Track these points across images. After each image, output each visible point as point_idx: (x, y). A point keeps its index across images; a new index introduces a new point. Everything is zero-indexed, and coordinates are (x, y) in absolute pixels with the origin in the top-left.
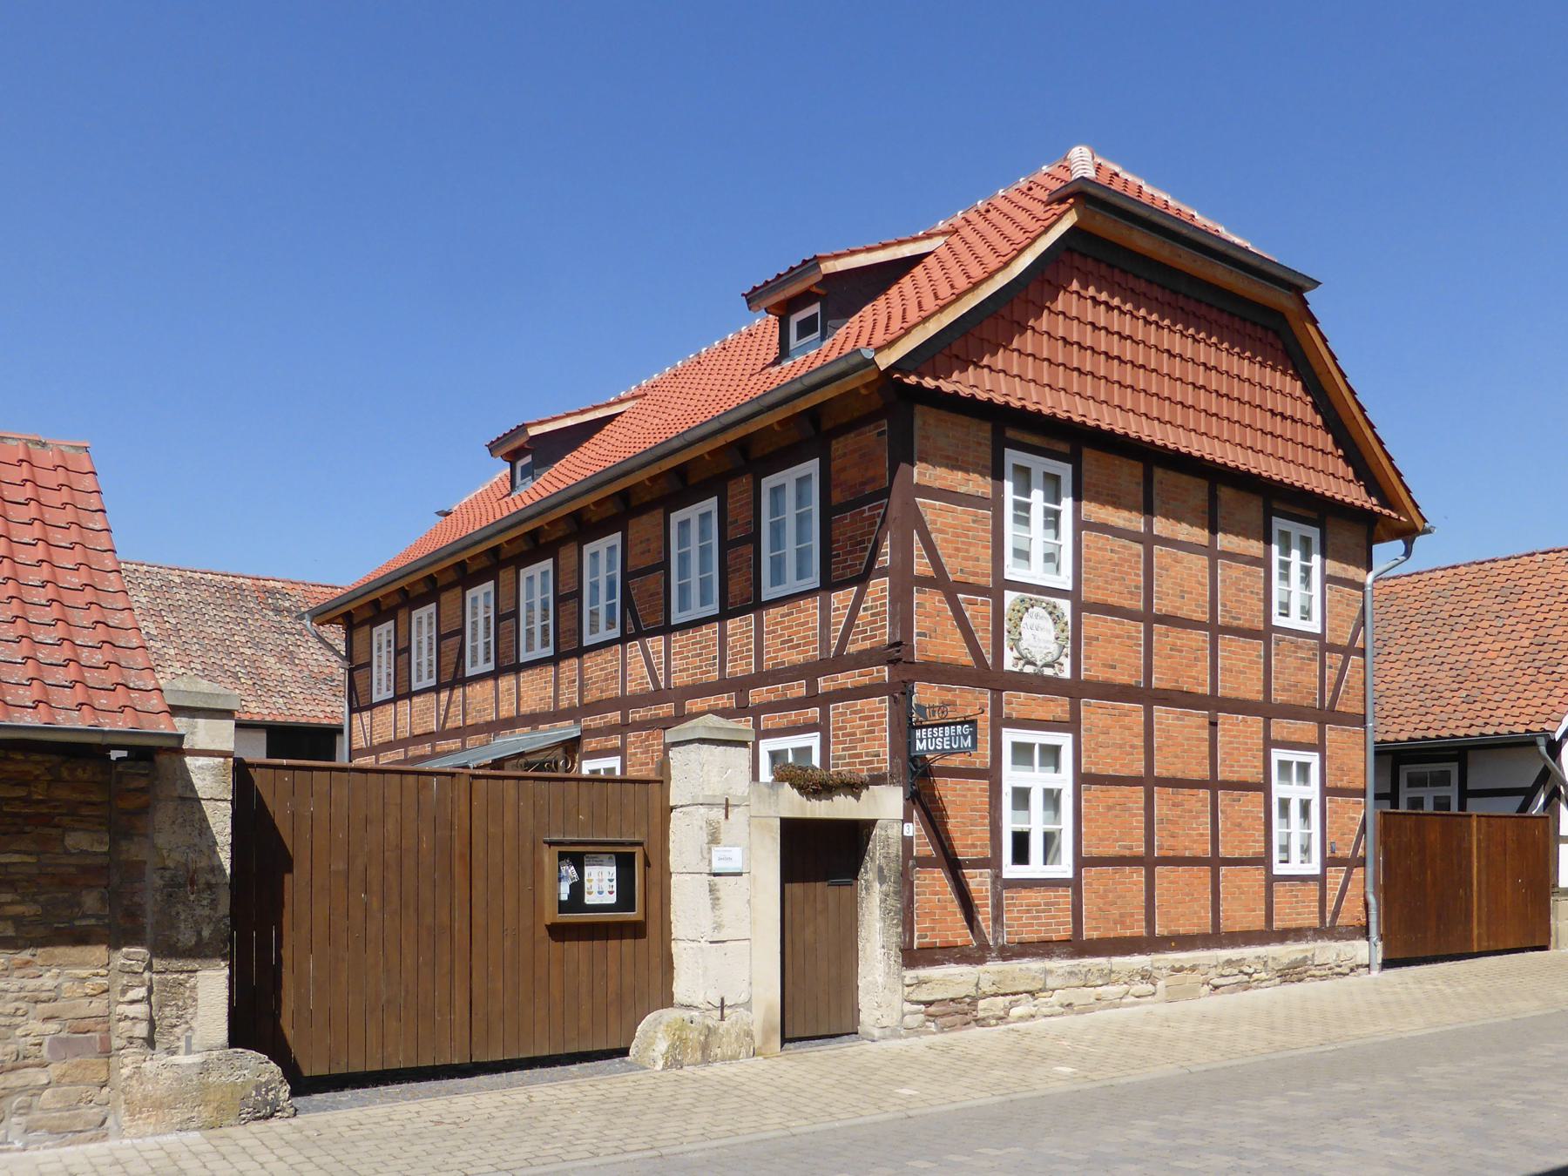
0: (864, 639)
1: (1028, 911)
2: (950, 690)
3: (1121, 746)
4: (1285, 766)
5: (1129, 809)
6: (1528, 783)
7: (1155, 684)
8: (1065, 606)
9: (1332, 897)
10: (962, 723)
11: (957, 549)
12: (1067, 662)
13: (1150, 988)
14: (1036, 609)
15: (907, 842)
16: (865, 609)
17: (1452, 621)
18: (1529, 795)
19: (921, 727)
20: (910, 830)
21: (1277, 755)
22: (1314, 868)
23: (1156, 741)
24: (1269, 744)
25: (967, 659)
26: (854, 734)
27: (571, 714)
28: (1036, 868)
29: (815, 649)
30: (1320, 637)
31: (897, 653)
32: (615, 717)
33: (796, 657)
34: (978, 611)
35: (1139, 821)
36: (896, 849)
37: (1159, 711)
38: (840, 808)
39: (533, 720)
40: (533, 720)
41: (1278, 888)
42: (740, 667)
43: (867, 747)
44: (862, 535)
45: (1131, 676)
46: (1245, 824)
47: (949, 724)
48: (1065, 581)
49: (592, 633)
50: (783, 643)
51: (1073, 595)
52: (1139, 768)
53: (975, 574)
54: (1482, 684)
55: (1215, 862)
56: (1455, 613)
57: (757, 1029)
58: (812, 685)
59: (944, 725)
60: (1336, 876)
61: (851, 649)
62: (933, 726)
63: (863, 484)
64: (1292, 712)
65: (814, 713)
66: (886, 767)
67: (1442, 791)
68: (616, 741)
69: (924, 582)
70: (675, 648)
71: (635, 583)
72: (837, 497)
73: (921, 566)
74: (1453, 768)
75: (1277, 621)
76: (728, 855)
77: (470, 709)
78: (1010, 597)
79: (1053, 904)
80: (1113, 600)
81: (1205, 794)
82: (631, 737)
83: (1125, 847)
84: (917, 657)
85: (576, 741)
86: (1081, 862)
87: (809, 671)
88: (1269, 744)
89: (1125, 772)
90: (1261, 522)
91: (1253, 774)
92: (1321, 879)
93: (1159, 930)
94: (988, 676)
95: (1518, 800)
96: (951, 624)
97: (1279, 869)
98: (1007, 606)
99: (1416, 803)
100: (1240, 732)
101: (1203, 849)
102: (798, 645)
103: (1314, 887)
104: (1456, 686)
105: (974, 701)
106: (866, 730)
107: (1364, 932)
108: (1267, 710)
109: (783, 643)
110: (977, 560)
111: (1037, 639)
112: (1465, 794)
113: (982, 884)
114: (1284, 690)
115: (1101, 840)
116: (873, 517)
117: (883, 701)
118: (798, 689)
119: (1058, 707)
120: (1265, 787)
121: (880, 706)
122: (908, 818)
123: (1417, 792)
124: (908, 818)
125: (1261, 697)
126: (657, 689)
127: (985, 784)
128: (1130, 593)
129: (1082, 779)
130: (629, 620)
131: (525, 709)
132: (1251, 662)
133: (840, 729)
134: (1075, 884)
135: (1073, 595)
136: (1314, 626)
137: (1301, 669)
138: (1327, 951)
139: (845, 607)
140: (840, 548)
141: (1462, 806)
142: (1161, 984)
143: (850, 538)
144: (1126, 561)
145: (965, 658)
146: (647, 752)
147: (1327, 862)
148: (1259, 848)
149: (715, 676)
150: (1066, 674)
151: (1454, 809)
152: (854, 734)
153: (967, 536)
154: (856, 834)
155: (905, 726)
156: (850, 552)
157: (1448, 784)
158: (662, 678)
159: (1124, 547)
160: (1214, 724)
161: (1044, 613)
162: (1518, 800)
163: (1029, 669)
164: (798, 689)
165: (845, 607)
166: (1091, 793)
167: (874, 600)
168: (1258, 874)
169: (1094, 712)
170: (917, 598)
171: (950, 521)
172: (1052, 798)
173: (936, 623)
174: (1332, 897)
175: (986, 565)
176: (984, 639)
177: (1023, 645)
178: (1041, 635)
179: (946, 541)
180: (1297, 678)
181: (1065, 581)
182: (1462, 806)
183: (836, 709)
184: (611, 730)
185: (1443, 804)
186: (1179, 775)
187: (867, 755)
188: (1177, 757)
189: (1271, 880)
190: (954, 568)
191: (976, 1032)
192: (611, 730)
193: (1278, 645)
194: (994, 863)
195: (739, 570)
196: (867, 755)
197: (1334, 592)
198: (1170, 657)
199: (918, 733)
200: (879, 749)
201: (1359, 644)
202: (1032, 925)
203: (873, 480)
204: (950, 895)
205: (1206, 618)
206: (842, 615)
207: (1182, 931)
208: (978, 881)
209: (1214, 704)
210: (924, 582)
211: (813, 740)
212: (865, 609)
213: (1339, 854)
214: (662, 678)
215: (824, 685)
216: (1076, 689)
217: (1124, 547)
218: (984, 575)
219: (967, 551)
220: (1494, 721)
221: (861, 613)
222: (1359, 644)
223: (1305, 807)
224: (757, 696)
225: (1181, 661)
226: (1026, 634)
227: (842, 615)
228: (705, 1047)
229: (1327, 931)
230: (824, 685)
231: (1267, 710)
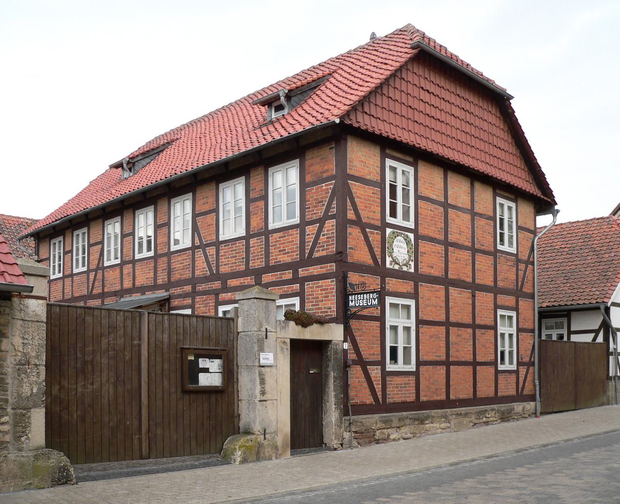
0: (322, 250)
1: (397, 387)
2: (363, 276)
3: (436, 307)
4: (502, 317)
5: (439, 338)
6: (597, 328)
7: (450, 276)
8: (411, 236)
9: (521, 380)
10: (373, 293)
11: (366, 207)
12: (412, 264)
13: (448, 425)
14: (399, 238)
15: (345, 351)
16: (323, 235)
17: (561, 250)
18: (596, 332)
19: (352, 295)
20: (346, 346)
21: (500, 312)
22: (514, 367)
23: (451, 304)
24: (496, 307)
25: (370, 261)
26: (318, 298)
27: (166, 287)
28: (400, 366)
29: (297, 255)
30: (516, 255)
31: (340, 256)
32: (188, 288)
33: (287, 259)
34: (375, 237)
35: (443, 344)
36: (340, 356)
37: (452, 290)
38: (313, 333)
39: (143, 290)
40: (143, 290)
41: (500, 377)
42: (257, 263)
43: (325, 304)
44: (322, 198)
45: (439, 272)
46: (487, 345)
47: (366, 293)
48: (411, 224)
49: (175, 245)
50: (280, 251)
51: (415, 231)
52: (443, 318)
53: (373, 219)
54: (576, 280)
55: (447, 364)
56: (563, 246)
57: (279, 444)
58: (296, 272)
59: (363, 293)
60: (523, 371)
61: (316, 255)
62: (358, 294)
63: (322, 173)
64: (506, 292)
65: (296, 287)
66: (334, 314)
67: (560, 331)
68: (189, 301)
69: (352, 222)
70: (222, 253)
71: (199, 219)
72: (308, 178)
73: (351, 215)
74: (565, 320)
75: (500, 247)
76: (267, 357)
77: (106, 283)
78: (389, 231)
79: (408, 384)
80: (431, 234)
81: (470, 331)
82: (198, 299)
83: (438, 356)
84: (350, 260)
85: (168, 300)
86: (419, 363)
87: (293, 266)
88: (496, 307)
89: (437, 319)
90: (492, 199)
91: (490, 322)
92: (517, 372)
93: (423, 398)
94: (379, 269)
95: (593, 335)
96: (363, 243)
97: (501, 367)
98: (387, 236)
99: (550, 336)
100: (485, 300)
101: (469, 358)
102: (288, 253)
103: (514, 376)
104: (565, 281)
105: (374, 282)
106: (323, 297)
107: (532, 398)
108: (495, 290)
109: (280, 251)
110: (375, 212)
111: (400, 252)
112: (570, 333)
113: (377, 373)
114: (502, 281)
115: (428, 352)
116: (328, 189)
117: (333, 281)
118: (288, 275)
119: (408, 287)
120: (495, 328)
121: (331, 284)
122: (345, 341)
123: (549, 332)
124: (345, 341)
125: (492, 284)
126: (212, 274)
127: (378, 324)
128: (439, 231)
129: (419, 322)
130: (197, 238)
131: (138, 284)
132: (488, 266)
133: (310, 295)
134: (416, 374)
135: (415, 231)
136: (513, 250)
137: (509, 271)
138: (518, 407)
139: (313, 234)
140: (310, 204)
141: (569, 338)
142: (452, 423)
143: (315, 199)
144: (437, 215)
145: (370, 261)
146: (206, 306)
147: (519, 364)
148: (492, 357)
149: (243, 268)
150: (412, 270)
151: (565, 339)
152: (318, 298)
153: (370, 200)
154: (321, 346)
155: (344, 295)
156: (315, 207)
157: (563, 328)
158: (214, 269)
159: (436, 209)
160: (474, 296)
161: (402, 239)
162: (593, 335)
163: (397, 267)
164: (288, 275)
165: (313, 234)
166: (424, 329)
167: (328, 231)
168: (491, 370)
169: (425, 290)
170: (349, 230)
171: (363, 192)
172: (407, 329)
173: (358, 243)
174: (521, 380)
175: (378, 216)
176: (377, 251)
177: (394, 255)
178: (402, 250)
179: (361, 202)
180: (507, 276)
181: (411, 224)
182: (569, 338)
183: (308, 285)
184: (185, 295)
185: (561, 337)
186: (460, 322)
187: (325, 308)
188: (459, 312)
189: (497, 372)
190: (365, 216)
191: (375, 447)
192: (185, 295)
193: (501, 259)
194: (382, 363)
195: (256, 214)
196: (325, 308)
197: (522, 234)
198: (456, 263)
199: (350, 298)
200: (330, 305)
201: (531, 259)
202: (398, 394)
203: (327, 171)
204: (363, 379)
205: (470, 245)
206: (312, 238)
207: (461, 397)
208: (375, 372)
209: (474, 287)
210: (352, 222)
211: (296, 301)
212: (323, 235)
213: (524, 360)
214: (214, 269)
215: (302, 273)
216: (417, 278)
217: (436, 209)
218: (377, 220)
219: (370, 208)
220: (583, 298)
221: (321, 237)
222: (531, 259)
223: (511, 336)
224: (267, 278)
225: (460, 266)
226: (395, 250)
227: (312, 238)
228: (258, 453)
229: (520, 397)
230: (302, 273)
231: (495, 290)
